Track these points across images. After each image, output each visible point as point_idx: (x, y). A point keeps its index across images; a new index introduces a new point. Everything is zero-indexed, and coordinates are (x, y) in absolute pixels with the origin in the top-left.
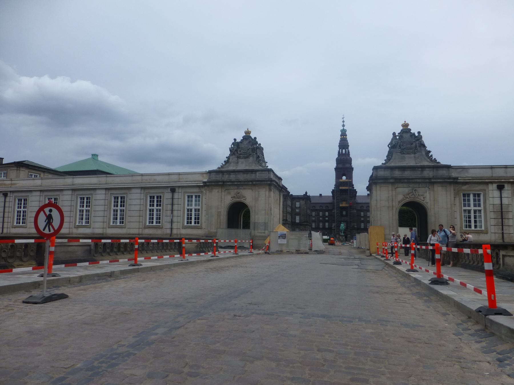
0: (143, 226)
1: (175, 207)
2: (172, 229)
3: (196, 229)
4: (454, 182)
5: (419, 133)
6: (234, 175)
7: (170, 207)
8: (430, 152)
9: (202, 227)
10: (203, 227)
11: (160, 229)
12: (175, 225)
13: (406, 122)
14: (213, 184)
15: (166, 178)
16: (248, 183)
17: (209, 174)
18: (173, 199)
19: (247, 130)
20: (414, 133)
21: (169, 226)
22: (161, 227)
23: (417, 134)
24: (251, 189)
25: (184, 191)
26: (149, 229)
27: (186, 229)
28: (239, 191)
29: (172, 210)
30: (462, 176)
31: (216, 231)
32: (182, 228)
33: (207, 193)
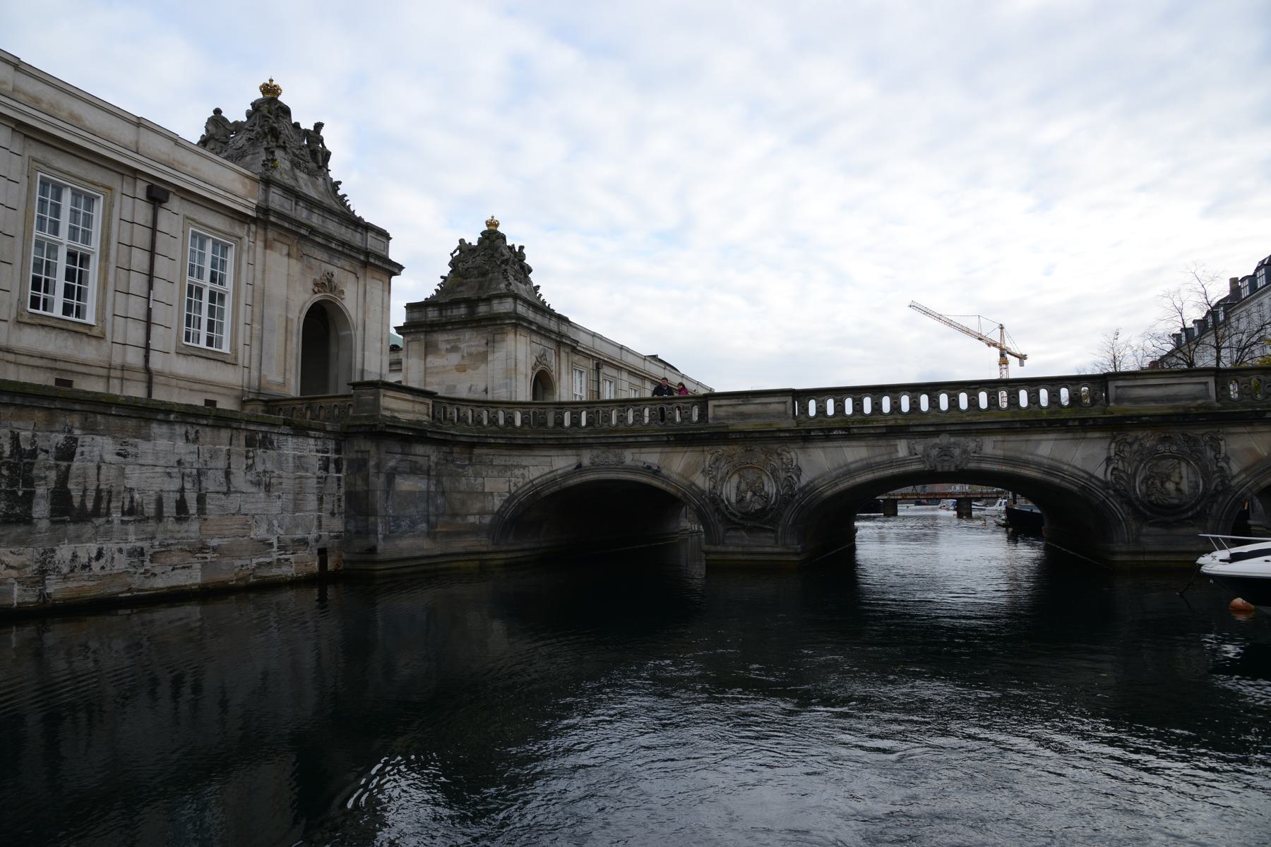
0: (13, 315)
1: (161, 265)
2: (147, 348)
3: (219, 364)
4: (574, 348)
5: (521, 248)
6: (320, 218)
7: (140, 259)
8: (538, 287)
9: (236, 358)
10: (240, 362)
11: (94, 342)
12: (159, 338)
13: (495, 219)
14: (286, 225)
15: (126, 134)
16: (357, 256)
17: (261, 186)
18: (154, 229)
19: (268, 82)
20: (513, 245)
21: (136, 334)
22: (95, 332)
23: (517, 250)
24: (356, 274)
25: (188, 214)
26: (42, 332)
27: (190, 358)
28: (330, 268)
29: (151, 276)
30: (584, 340)
31: (280, 380)
32: (178, 353)
33: (257, 248)
